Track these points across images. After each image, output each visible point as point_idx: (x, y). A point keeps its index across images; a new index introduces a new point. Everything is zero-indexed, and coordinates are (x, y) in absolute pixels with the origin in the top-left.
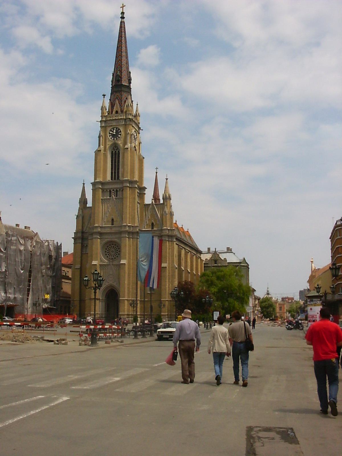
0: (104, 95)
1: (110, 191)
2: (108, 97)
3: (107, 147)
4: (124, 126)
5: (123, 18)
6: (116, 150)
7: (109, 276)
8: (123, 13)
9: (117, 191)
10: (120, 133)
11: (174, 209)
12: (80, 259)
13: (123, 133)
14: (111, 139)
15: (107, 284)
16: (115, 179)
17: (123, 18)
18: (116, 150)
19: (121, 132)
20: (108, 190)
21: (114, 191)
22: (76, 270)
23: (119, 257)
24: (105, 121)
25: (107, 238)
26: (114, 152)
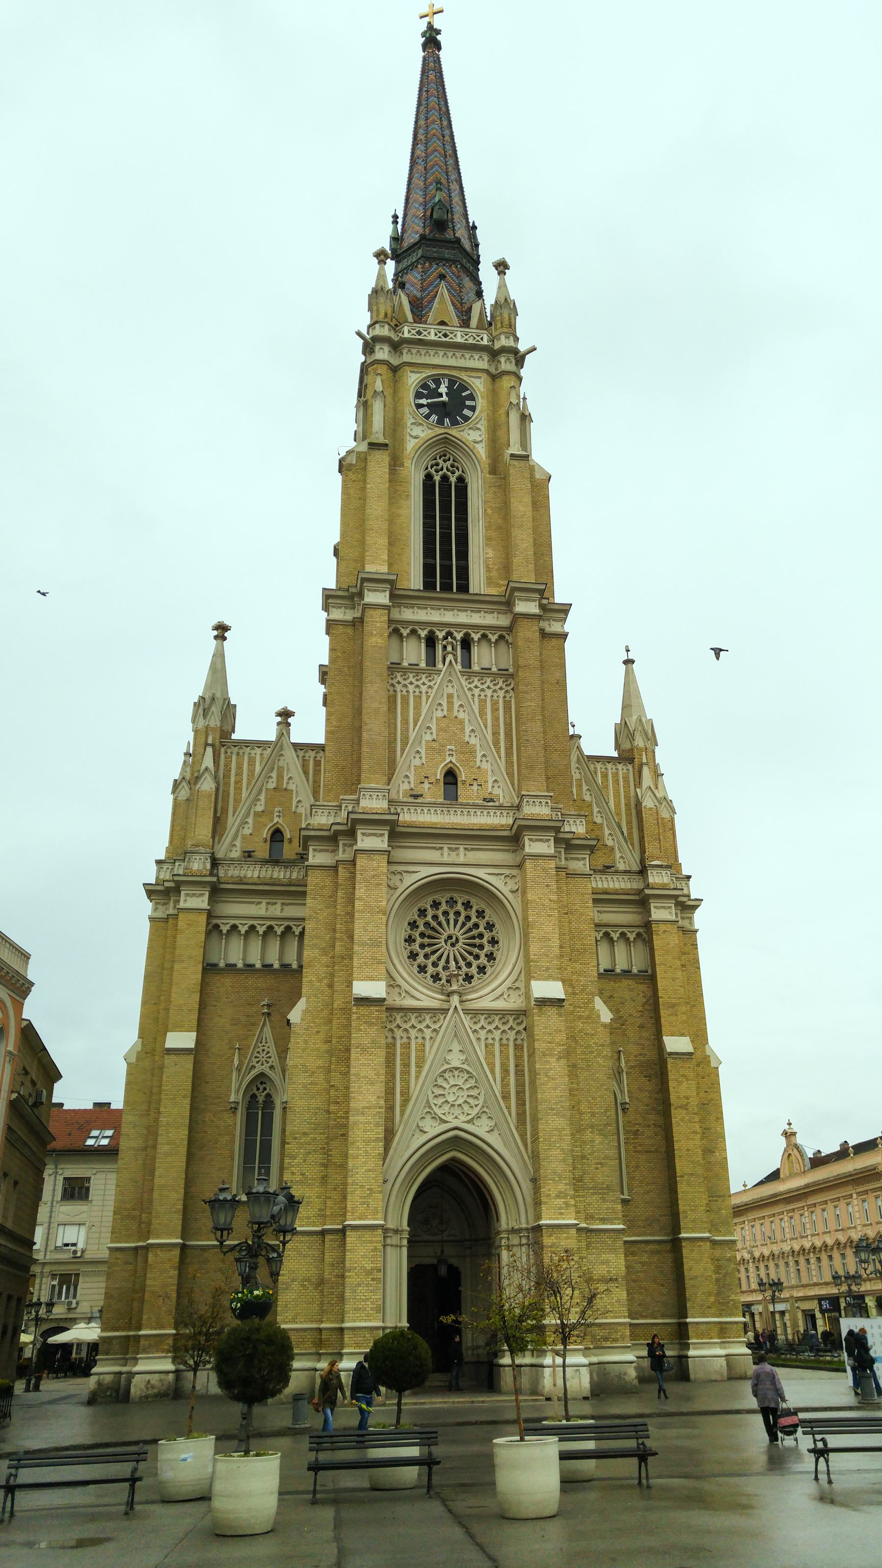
3: (410, 445)
4: (484, 376)
6: (445, 470)
7: (440, 1081)
10: (468, 403)
11: (674, 786)
12: (196, 997)
13: (481, 403)
14: (427, 417)
15: (432, 1129)
18: (445, 470)
19: (472, 397)
20: (423, 634)
21: (455, 638)
22: (173, 1058)
23: (489, 970)
26: (437, 478)
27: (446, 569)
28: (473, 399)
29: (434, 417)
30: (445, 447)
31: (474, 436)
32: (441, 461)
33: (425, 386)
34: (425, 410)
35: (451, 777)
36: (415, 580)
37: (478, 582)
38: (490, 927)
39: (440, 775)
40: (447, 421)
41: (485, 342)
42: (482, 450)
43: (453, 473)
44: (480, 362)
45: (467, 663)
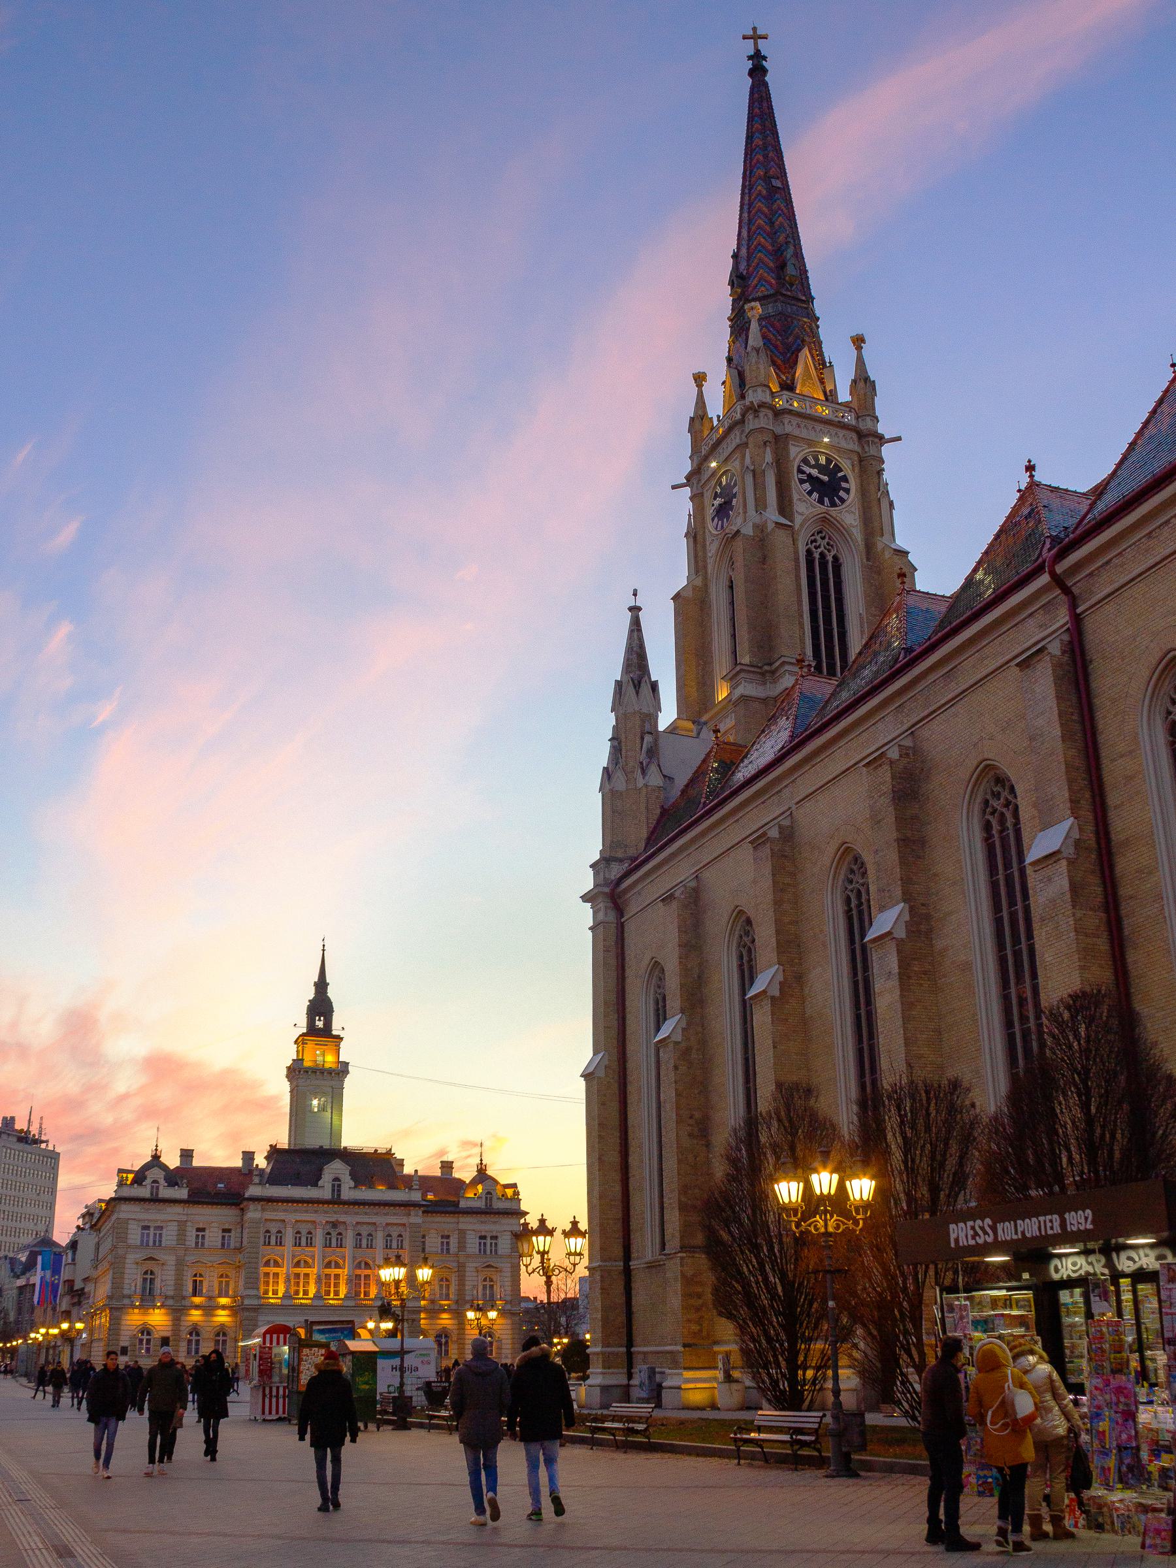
5: (758, 70)
6: (822, 548)
10: (844, 485)
13: (853, 485)
14: (810, 493)
17: (758, 70)
18: (822, 548)
24: (778, 413)
26: (817, 556)
28: (847, 481)
29: (815, 495)
30: (826, 526)
31: (849, 515)
32: (818, 538)
33: (805, 461)
34: (807, 486)
40: (826, 500)
42: (858, 535)
43: (829, 551)
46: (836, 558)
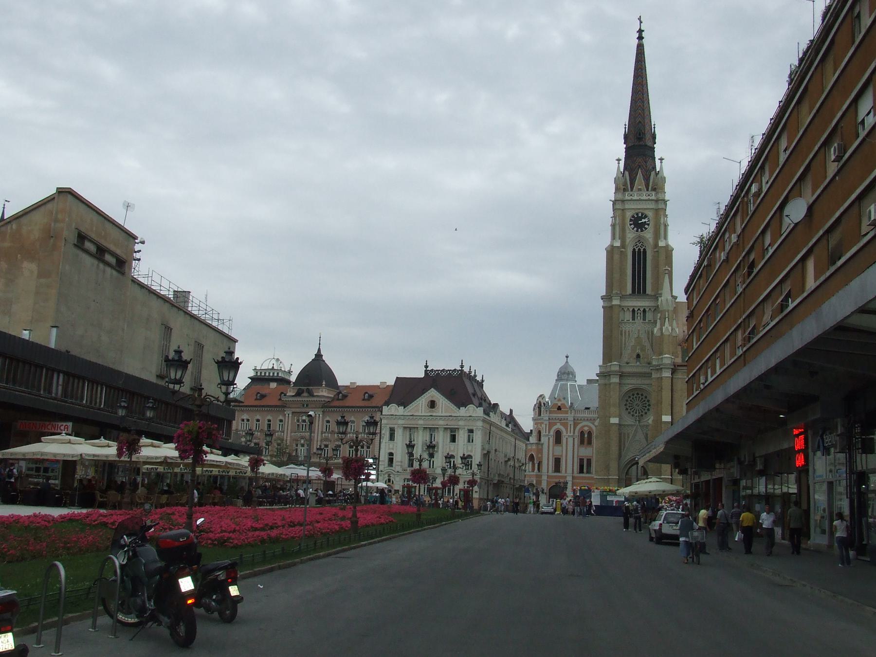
0: (619, 160)
1: (633, 311)
2: (622, 163)
3: (628, 241)
5: (640, 38)
8: (640, 31)
9: (644, 311)
16: (639, 292)
17: (640, 38)
24: (623, 201)
25: (631, 383)
27: (639, 288)
30: (640, 240)
31: (648, 234)
33: (633, 216)
35: (638, 356)
36: (629, 290)
37: (649, 290)
38: (648, 401)
39: (635, 356)
41: (653, 197)
42: (651, 241)
44: (652, 205)
45: (644, 319)
46: (644, 249)
